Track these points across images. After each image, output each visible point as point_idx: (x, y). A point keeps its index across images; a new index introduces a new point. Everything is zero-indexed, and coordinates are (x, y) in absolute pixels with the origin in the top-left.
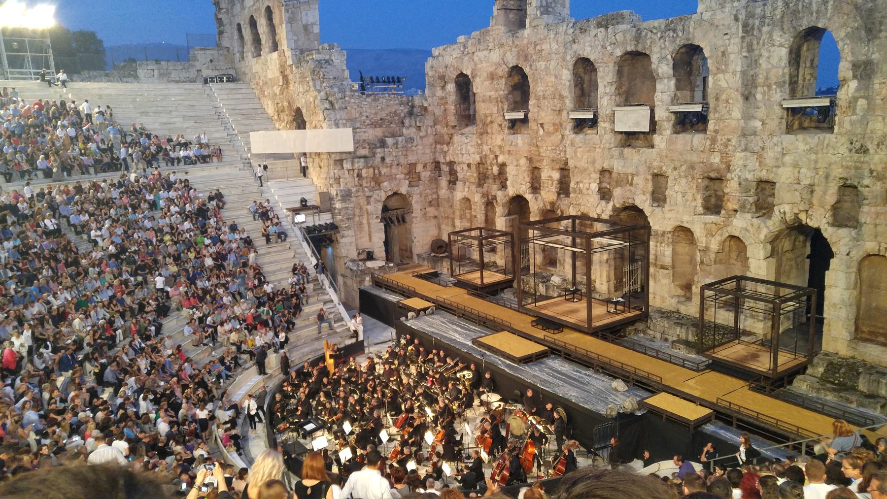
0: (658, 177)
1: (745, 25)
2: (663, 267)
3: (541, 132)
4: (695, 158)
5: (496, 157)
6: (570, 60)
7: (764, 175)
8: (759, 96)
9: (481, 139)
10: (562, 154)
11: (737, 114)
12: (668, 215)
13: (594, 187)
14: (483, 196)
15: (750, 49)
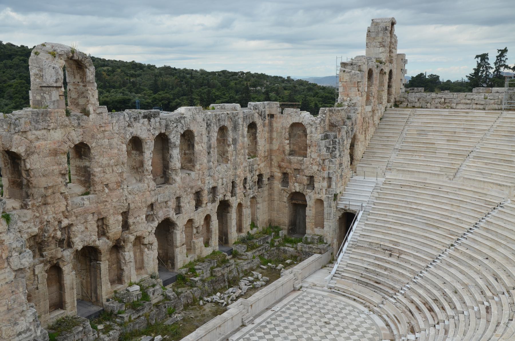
0: (178, 199)
1: (207, 123)
2: (183, 245)
3: (107, 190)
4: (193, 185)
5: (60, 222)
6: (129, 137)
7: (215, 185)
8: (212, 152)
9: (38, 211)
10: (125, 201)
11: (206, 161)
12: (185, 216)
13: (145, 216)
14: (45, 263)
15: (209, 133)
